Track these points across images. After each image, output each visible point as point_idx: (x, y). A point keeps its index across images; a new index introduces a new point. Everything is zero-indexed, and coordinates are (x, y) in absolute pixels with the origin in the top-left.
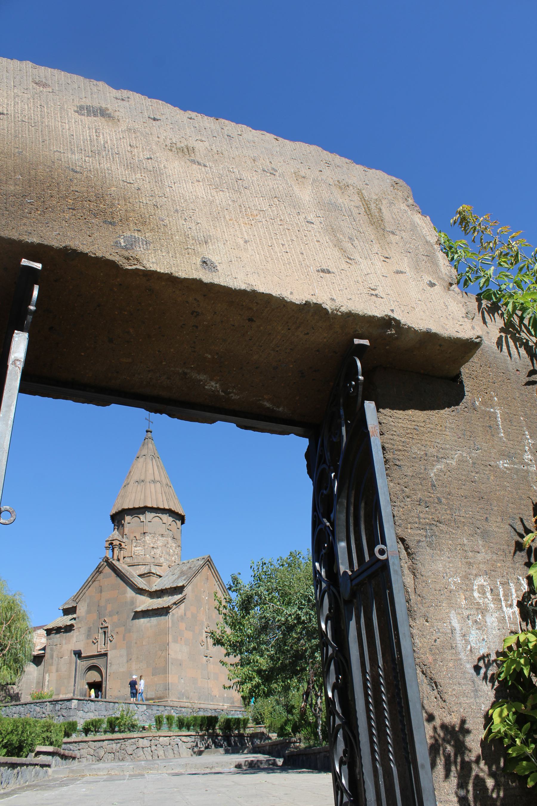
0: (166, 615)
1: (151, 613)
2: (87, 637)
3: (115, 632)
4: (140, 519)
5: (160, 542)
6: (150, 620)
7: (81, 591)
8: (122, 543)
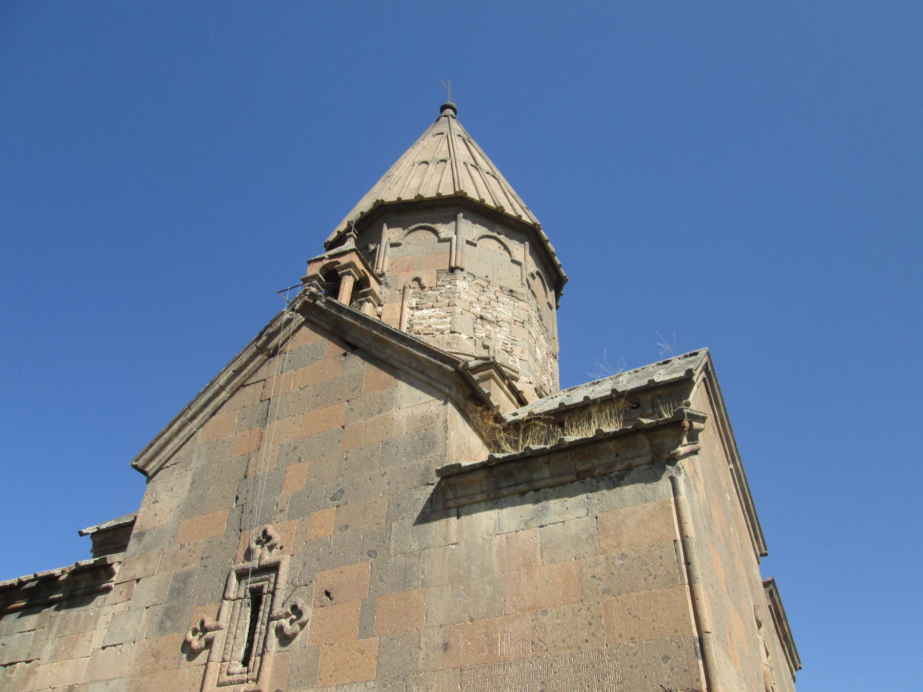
0: (656, 478)
1: (544, 473)
2: (162, 622)
3: (317, 588)
4: (435, 232)
5: (505, 309)
6: (544, 512)
7: (176, 427)
8: (372, 279)
